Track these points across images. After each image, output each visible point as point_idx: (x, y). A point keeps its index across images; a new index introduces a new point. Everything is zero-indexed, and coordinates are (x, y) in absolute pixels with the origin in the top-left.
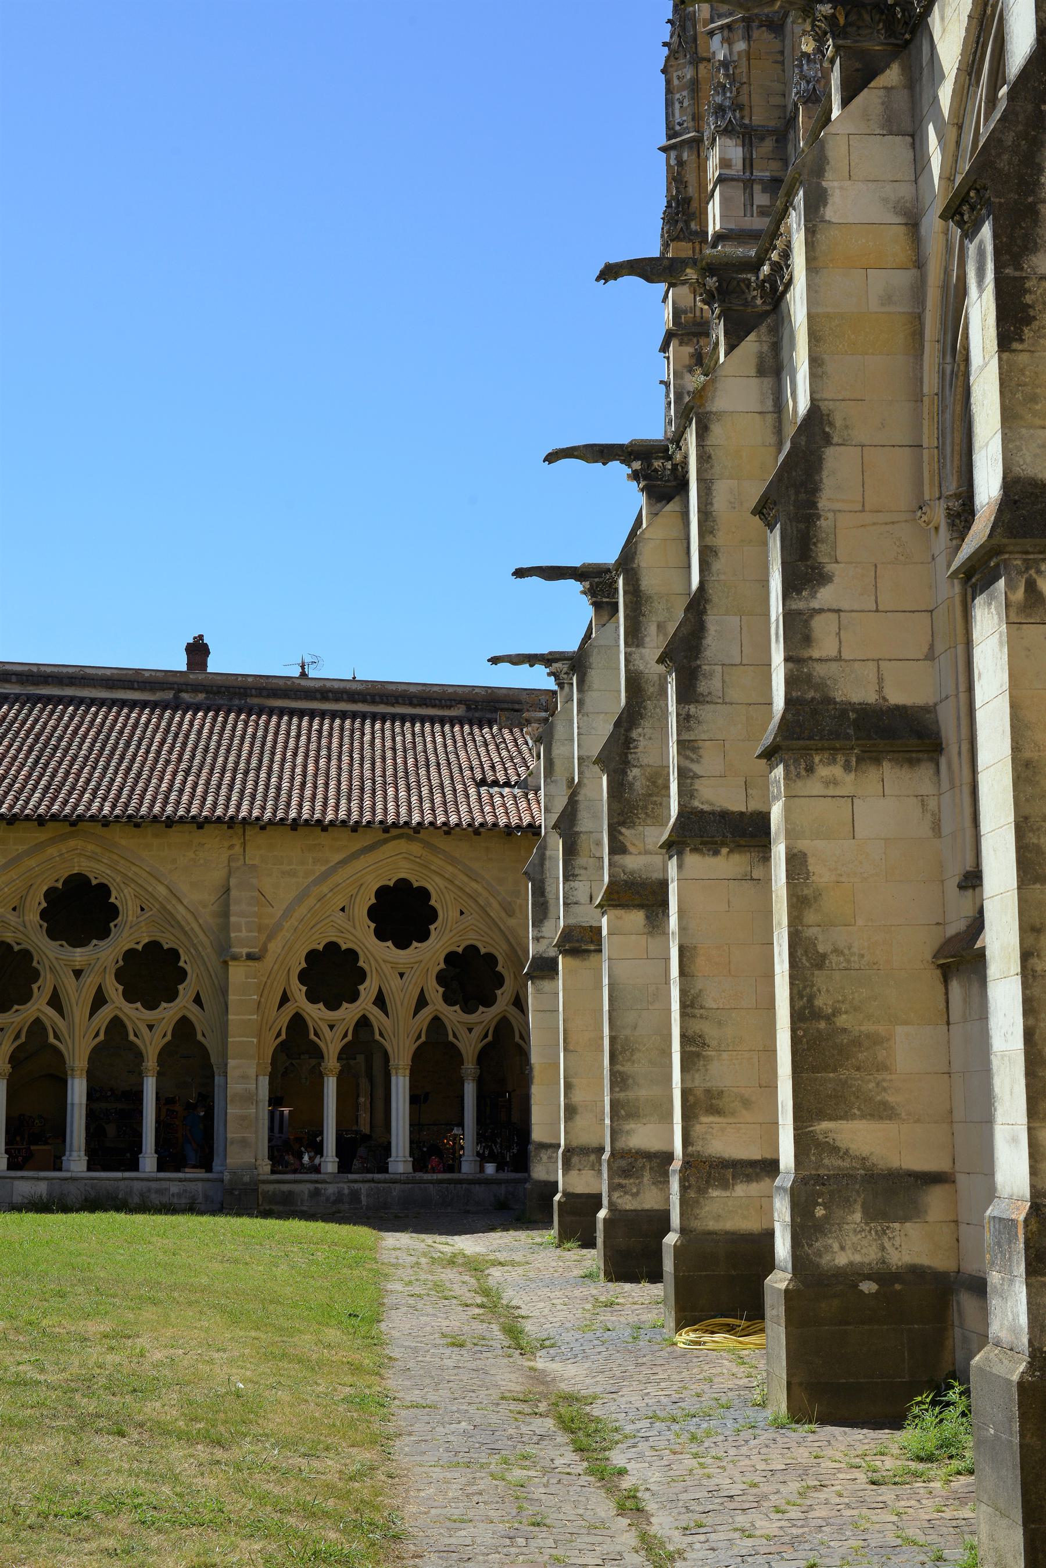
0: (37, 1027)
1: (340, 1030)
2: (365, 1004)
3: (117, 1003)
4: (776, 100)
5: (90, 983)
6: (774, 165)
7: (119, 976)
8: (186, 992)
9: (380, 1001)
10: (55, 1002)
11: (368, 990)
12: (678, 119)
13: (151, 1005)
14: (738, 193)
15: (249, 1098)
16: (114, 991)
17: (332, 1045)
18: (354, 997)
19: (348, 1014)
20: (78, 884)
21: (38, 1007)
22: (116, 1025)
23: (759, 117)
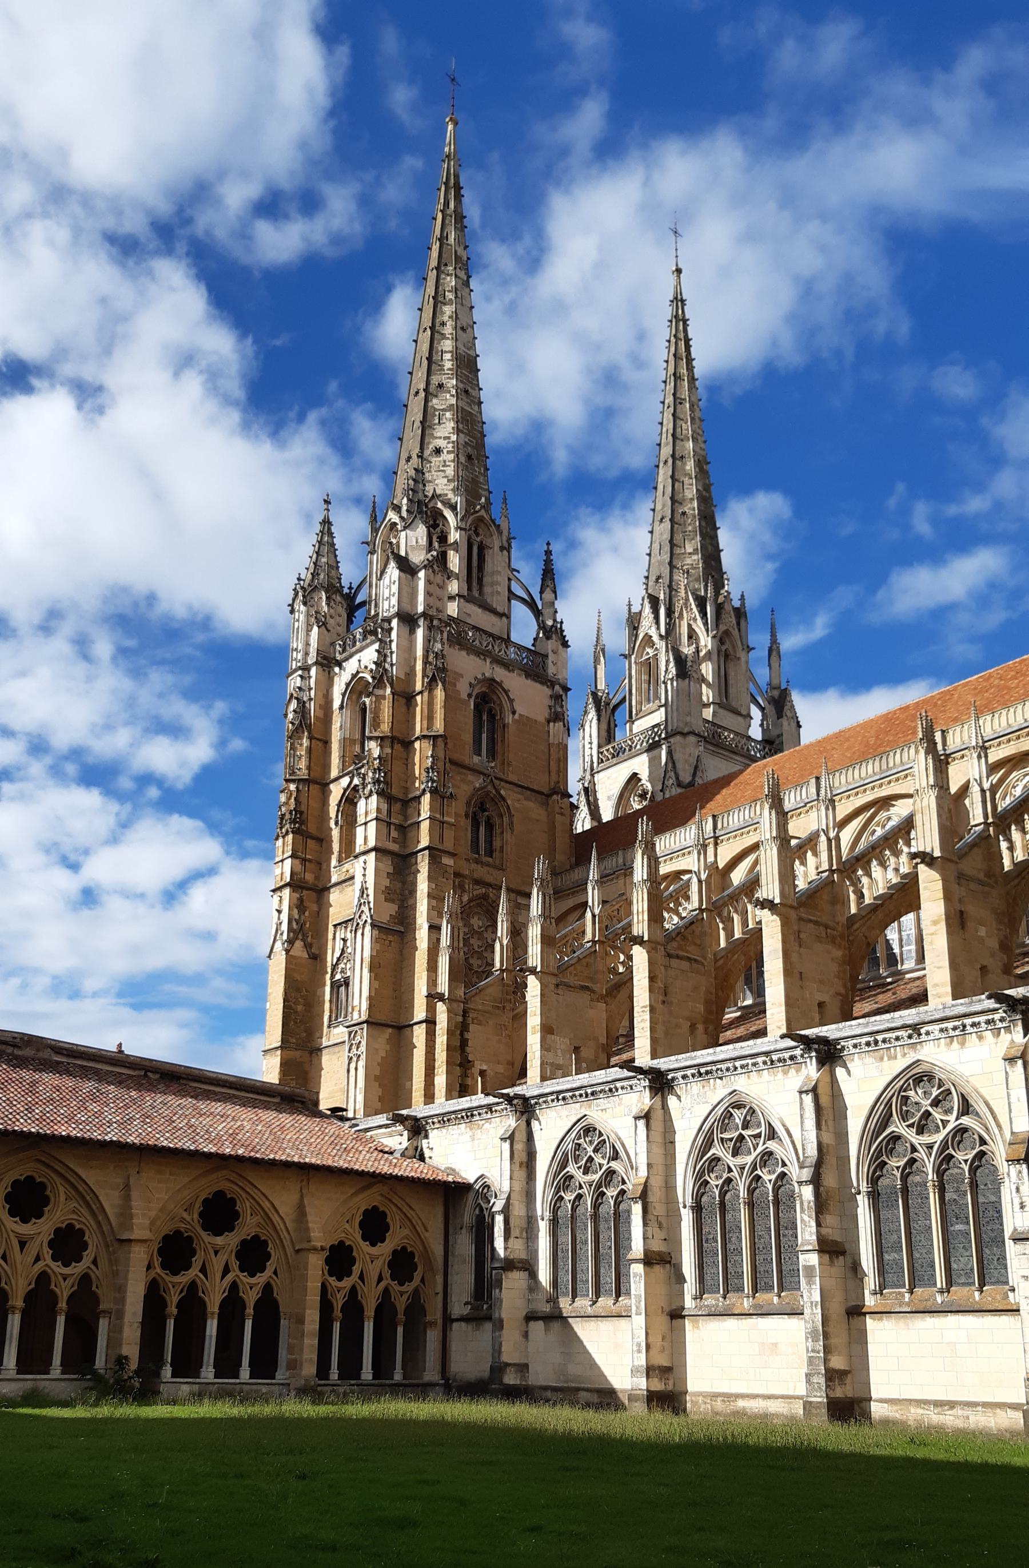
4: (403, 784)
6: (401, 817)
7: (238, 1256)
10: (203, 1270)
16: (235, 1264)
21: (194, 1272)
22: (234, 1286)
23: (395, 791)
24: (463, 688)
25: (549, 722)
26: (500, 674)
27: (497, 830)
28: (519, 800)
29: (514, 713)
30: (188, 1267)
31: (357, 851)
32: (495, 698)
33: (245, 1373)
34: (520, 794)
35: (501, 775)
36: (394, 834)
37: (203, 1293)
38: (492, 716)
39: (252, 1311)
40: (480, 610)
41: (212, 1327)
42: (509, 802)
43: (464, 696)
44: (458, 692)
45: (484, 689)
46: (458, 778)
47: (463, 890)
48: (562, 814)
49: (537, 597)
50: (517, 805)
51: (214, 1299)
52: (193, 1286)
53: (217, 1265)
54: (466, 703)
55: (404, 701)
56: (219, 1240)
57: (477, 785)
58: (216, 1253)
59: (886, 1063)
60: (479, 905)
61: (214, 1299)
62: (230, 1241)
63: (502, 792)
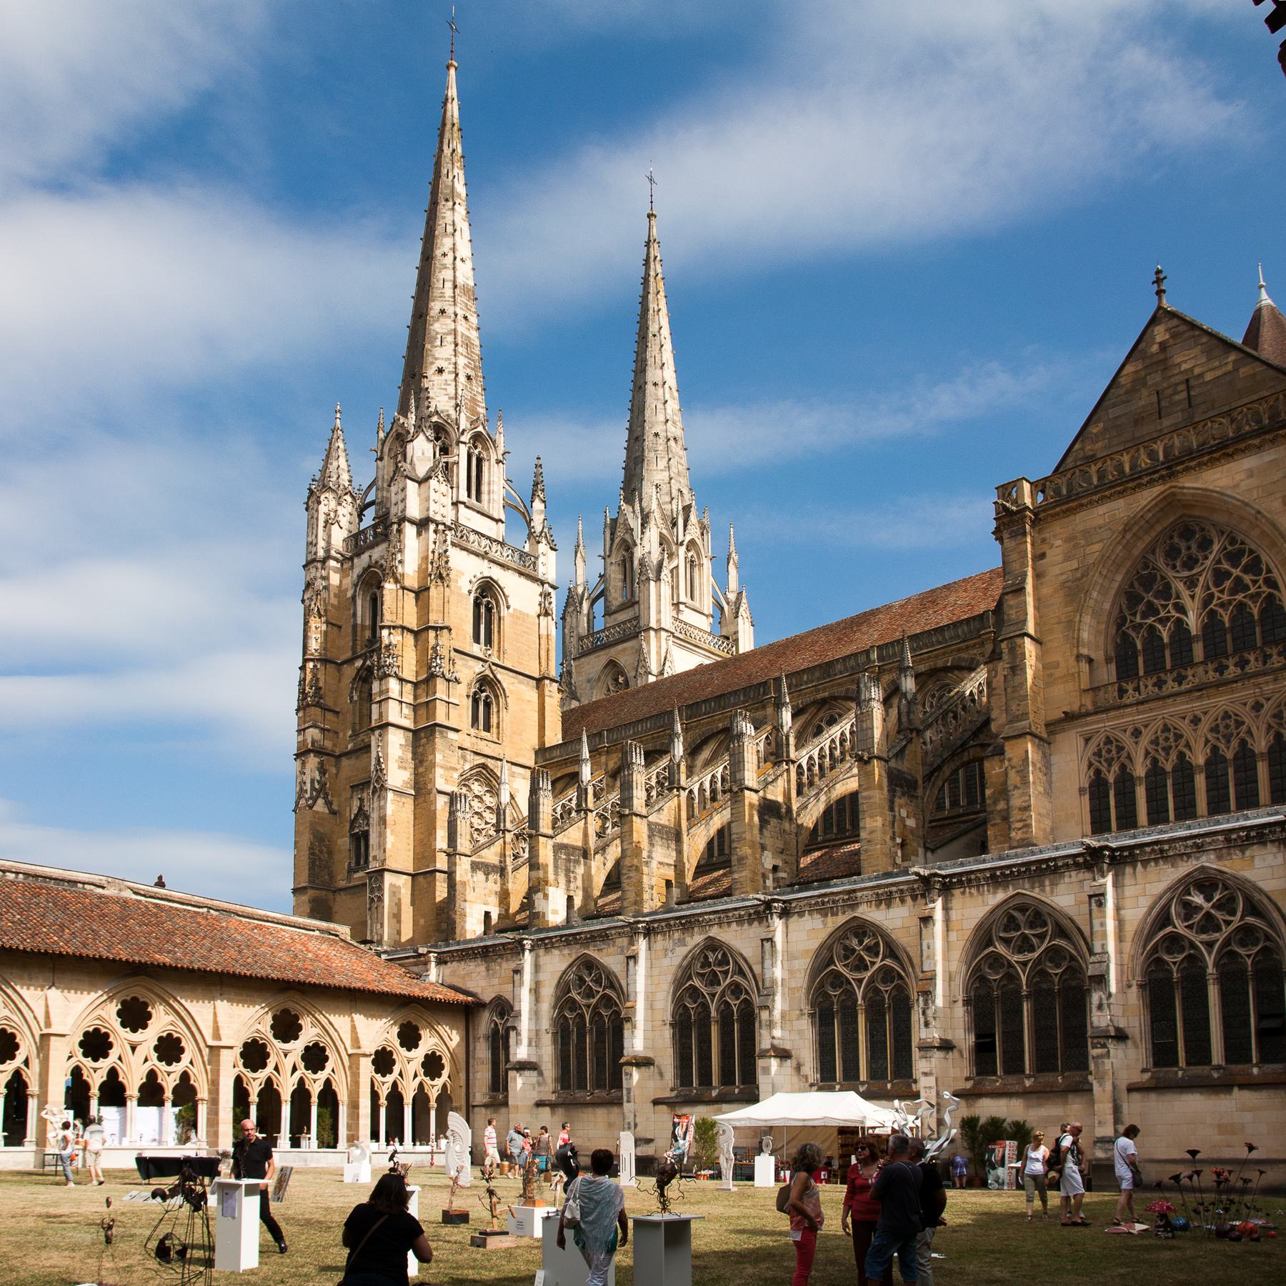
25: (539, 616)
26: (496, 573)
27: (494, 708)
29: (508, 607)
30: (264, 1066)
31: (373, 724)
35: (497, 661)
38: (489, 610)
39: (317, 1100)
42: (505, 685)
47: (465, 760)
48: (550, 696)
49: (528, 507)
50: (512, 688)
52: (269, 1081)
56: (287, 1046)
57: (478, 671)
58: (286, 1056)
59: (830, 919)
60: (479, 774)
62: (296, 1047)
63: (499, 676)
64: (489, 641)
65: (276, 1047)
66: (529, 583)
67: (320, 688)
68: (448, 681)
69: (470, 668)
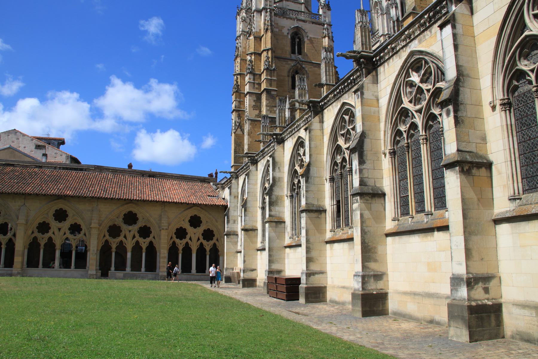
0: (121, 242)
1: (182, 245)
2: (187, 239)
3: (137, 237)
5: (132, 233)
8: (152, 236)
9: (190, 239)
10: (125, 237)
11: (188, 237)
12: (237, 70)
13: (145, 238)
14: (252, 85)
15: (164, 257)
16: (137, 235)
17: (181, 248)
18: (185, 238)
19: (184, 241)
20: (130, 213)
21: (121, 238)
22: (137, 243)
24: (285, 31)
26: (300, 24)
28: (311, 68)
29: (308, 37)
30: (119, 236)
32: (300, 32)
33: (143, 269)
34: (311, 65)
36: (256, 86)
37: (133, 244)
40: (293, 3)
41: (129, 255)
42: (306, 69)
43: (286, 34)
44: (283, 33)
45: (295, 30)
46: (284, 63)
50: (310, 69)
51: (129, 245)
52: (121, 242)
53: (130, 236)
54: (287, 36)
55: (259, 39)
56: (130, 228)
57: (293, 65)
61: (129, 245)
62: (135, 228)
63: (303, 66)
64: (300, 53)
65: (125, 228)
66: (318, 26)
67: (238, 85)
68: (271, 70)
69: (289, 64)
